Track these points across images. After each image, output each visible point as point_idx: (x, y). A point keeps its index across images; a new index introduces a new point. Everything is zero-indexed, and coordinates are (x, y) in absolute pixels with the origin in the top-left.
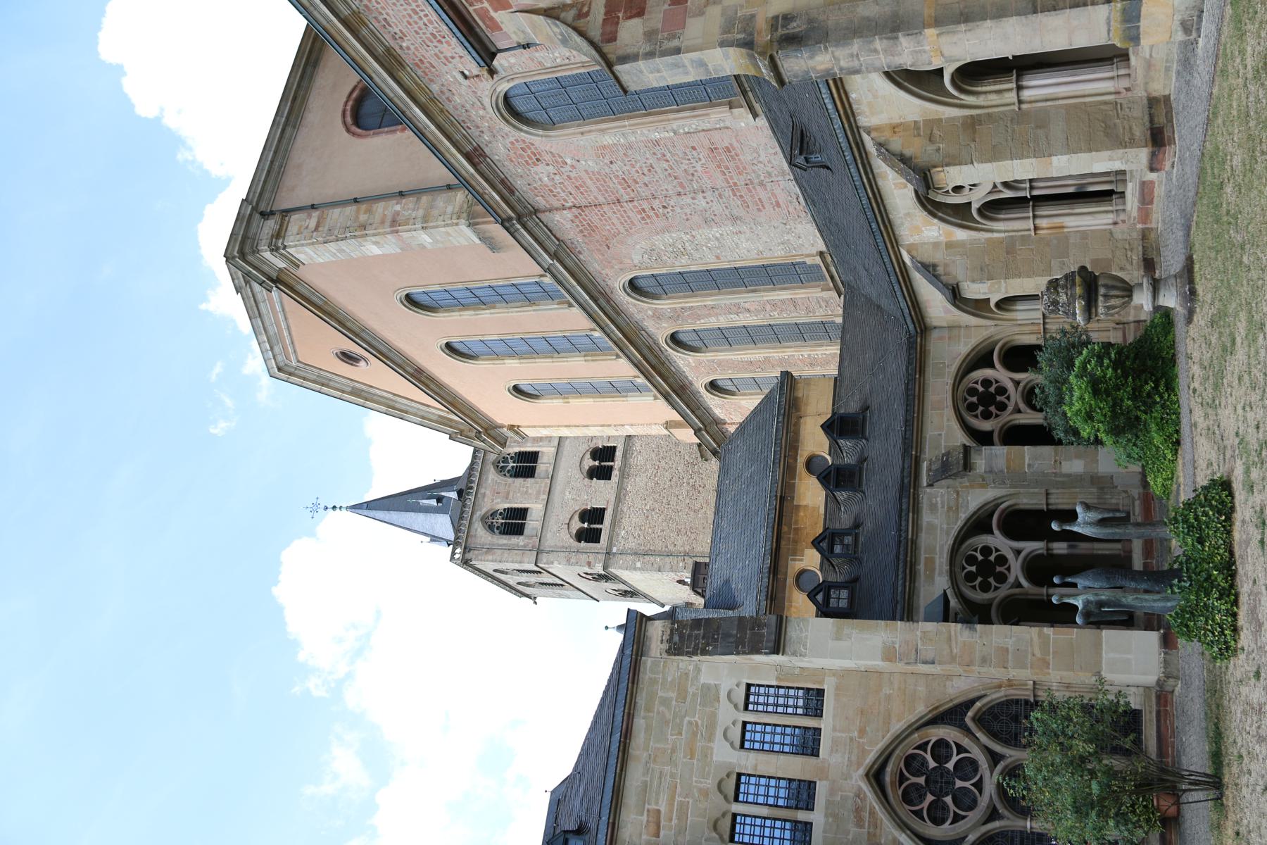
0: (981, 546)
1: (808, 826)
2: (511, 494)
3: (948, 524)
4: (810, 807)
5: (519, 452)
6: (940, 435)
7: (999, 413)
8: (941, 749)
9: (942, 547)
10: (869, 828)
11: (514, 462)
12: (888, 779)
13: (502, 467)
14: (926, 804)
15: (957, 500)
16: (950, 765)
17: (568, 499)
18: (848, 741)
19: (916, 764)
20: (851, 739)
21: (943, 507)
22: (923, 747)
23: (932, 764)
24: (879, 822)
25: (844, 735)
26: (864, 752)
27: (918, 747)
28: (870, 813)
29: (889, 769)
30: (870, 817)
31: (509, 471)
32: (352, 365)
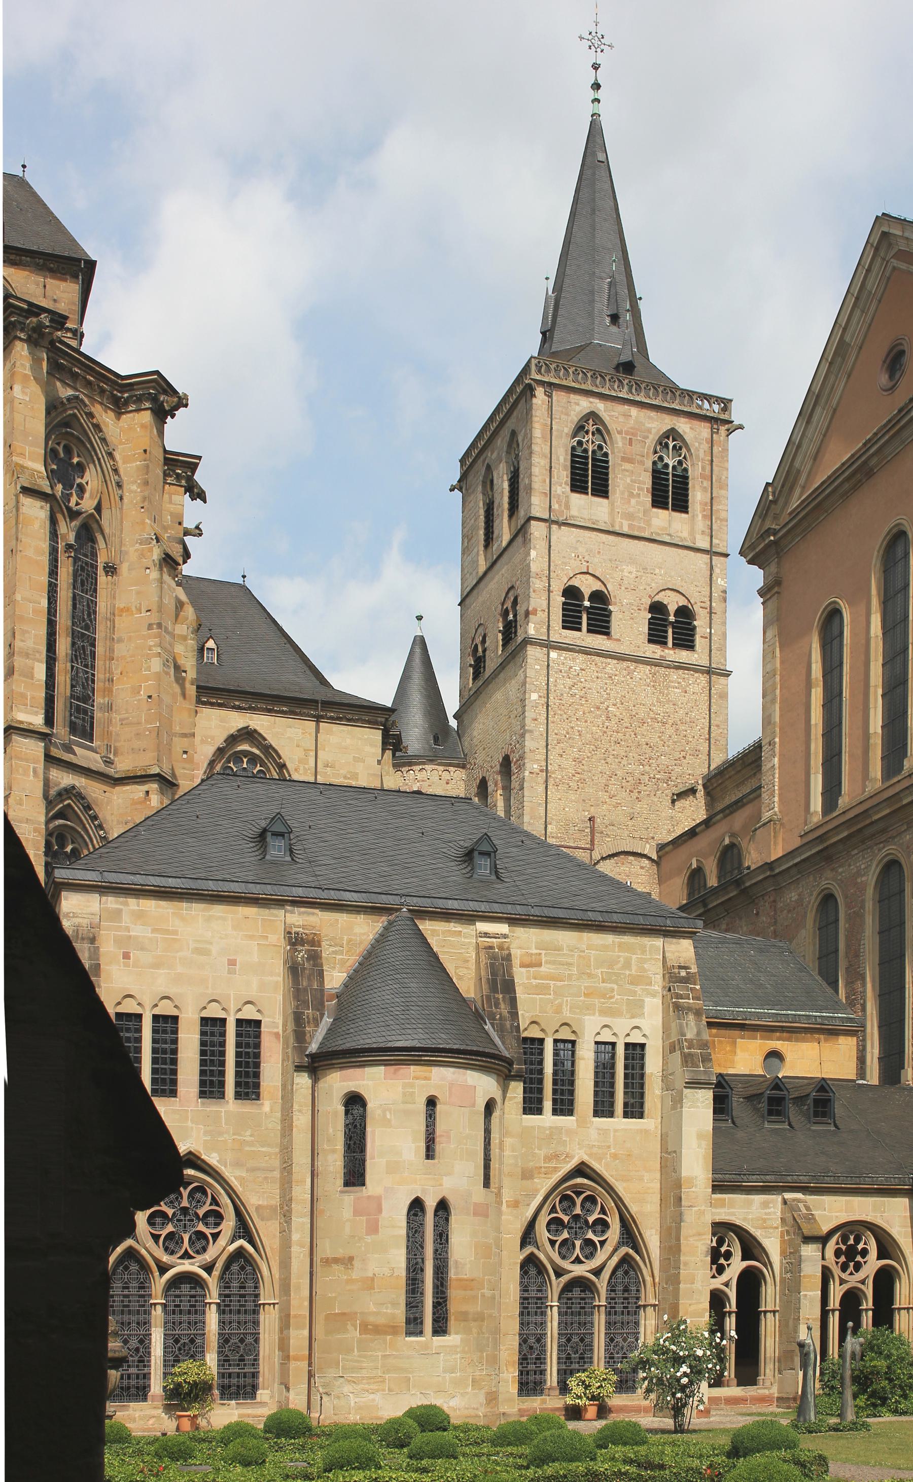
0: (732, 1250)
1: (539, 1111)
2: (627, 466)
3: (752, 1219)
4: (555, 1112)
5: (687, 478)
6: (825, 1210)
7: (840, 1264)
8: (602, 1225)
9: (733, 1214)
10: (544, 1167)
11: (674, 467)
12: (580, 1180)
13: (667, 445)
14: (561, 1215)
15: (771, 1228)
16: (590, 1235)
17: (622, 571)
18: (608, 1144)
19: (588, 1204)
20: (609, 1147)
21: (766, 1214)
22: (603, 1211)
23: (591, 1219)
24: (550, 1176)
25: (611, 1140)
26: (599, 1160)
27: (602, 1207)
28: (555, 1168)
29: (586, 1181)
30: (552, 1167)
31: (661, 458)
32: (884, 362)
